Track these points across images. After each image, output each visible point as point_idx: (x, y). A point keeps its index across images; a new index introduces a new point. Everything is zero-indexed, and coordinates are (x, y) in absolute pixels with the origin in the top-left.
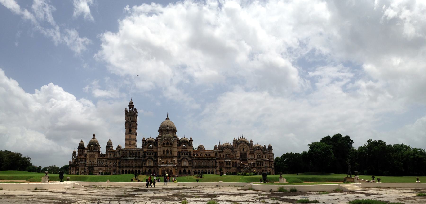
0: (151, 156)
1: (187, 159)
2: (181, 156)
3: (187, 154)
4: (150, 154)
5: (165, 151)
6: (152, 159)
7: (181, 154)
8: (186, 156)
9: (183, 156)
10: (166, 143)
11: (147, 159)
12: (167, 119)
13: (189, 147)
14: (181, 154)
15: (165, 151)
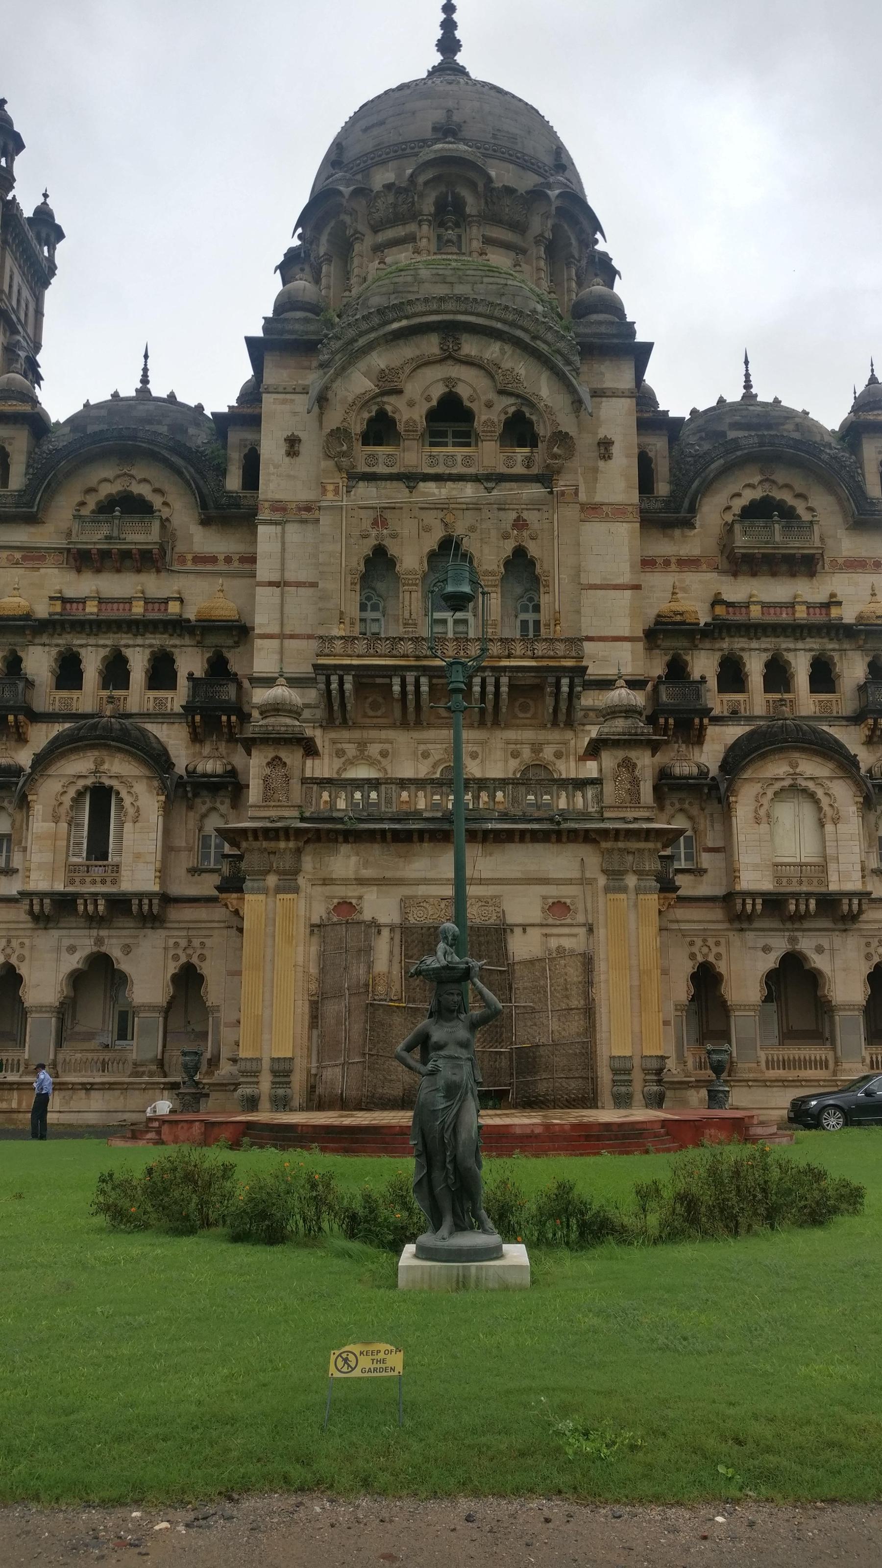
0: (137, 696)
1: (846, 764)
2: (717, 701)
3: (823, 677)
4: (116, 672)
5: (411, 558)
6: (157, 760)
7: (704, 665)
8: (805, 700)
9: (757, 699)
10: (411, 409)
11: (44, 760)
12: (448, 68)
13: (848, 545)
14: (704, 665)
15: (411, 558)
